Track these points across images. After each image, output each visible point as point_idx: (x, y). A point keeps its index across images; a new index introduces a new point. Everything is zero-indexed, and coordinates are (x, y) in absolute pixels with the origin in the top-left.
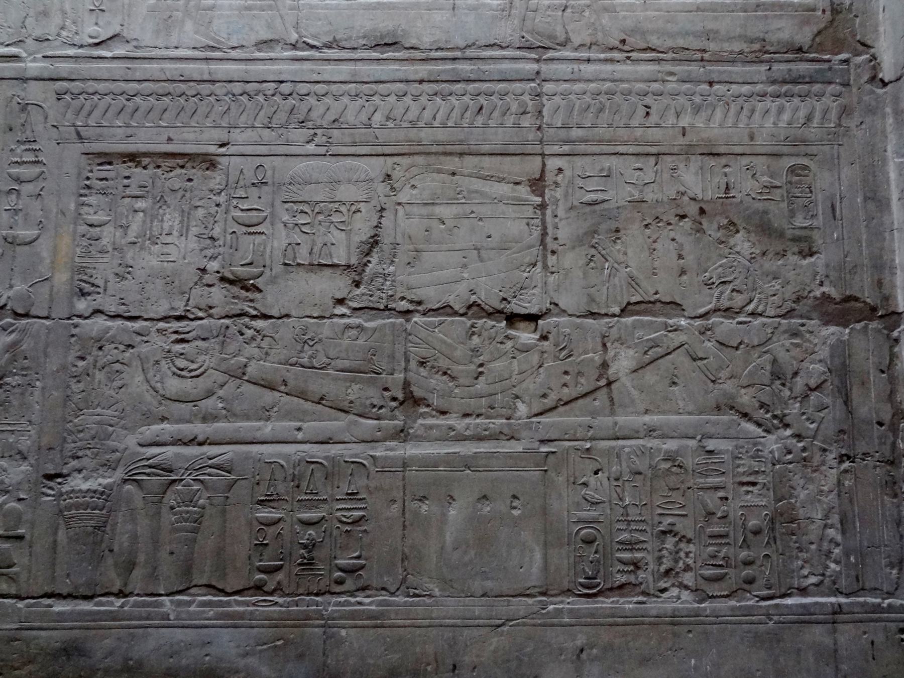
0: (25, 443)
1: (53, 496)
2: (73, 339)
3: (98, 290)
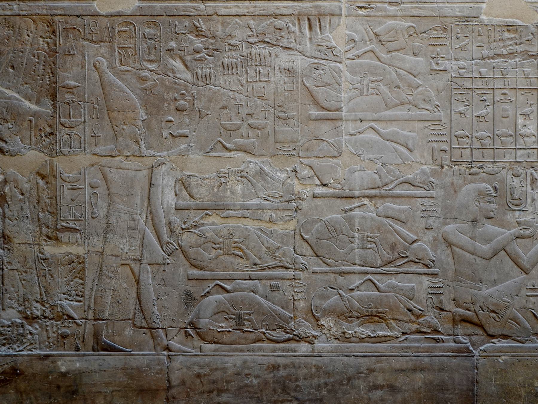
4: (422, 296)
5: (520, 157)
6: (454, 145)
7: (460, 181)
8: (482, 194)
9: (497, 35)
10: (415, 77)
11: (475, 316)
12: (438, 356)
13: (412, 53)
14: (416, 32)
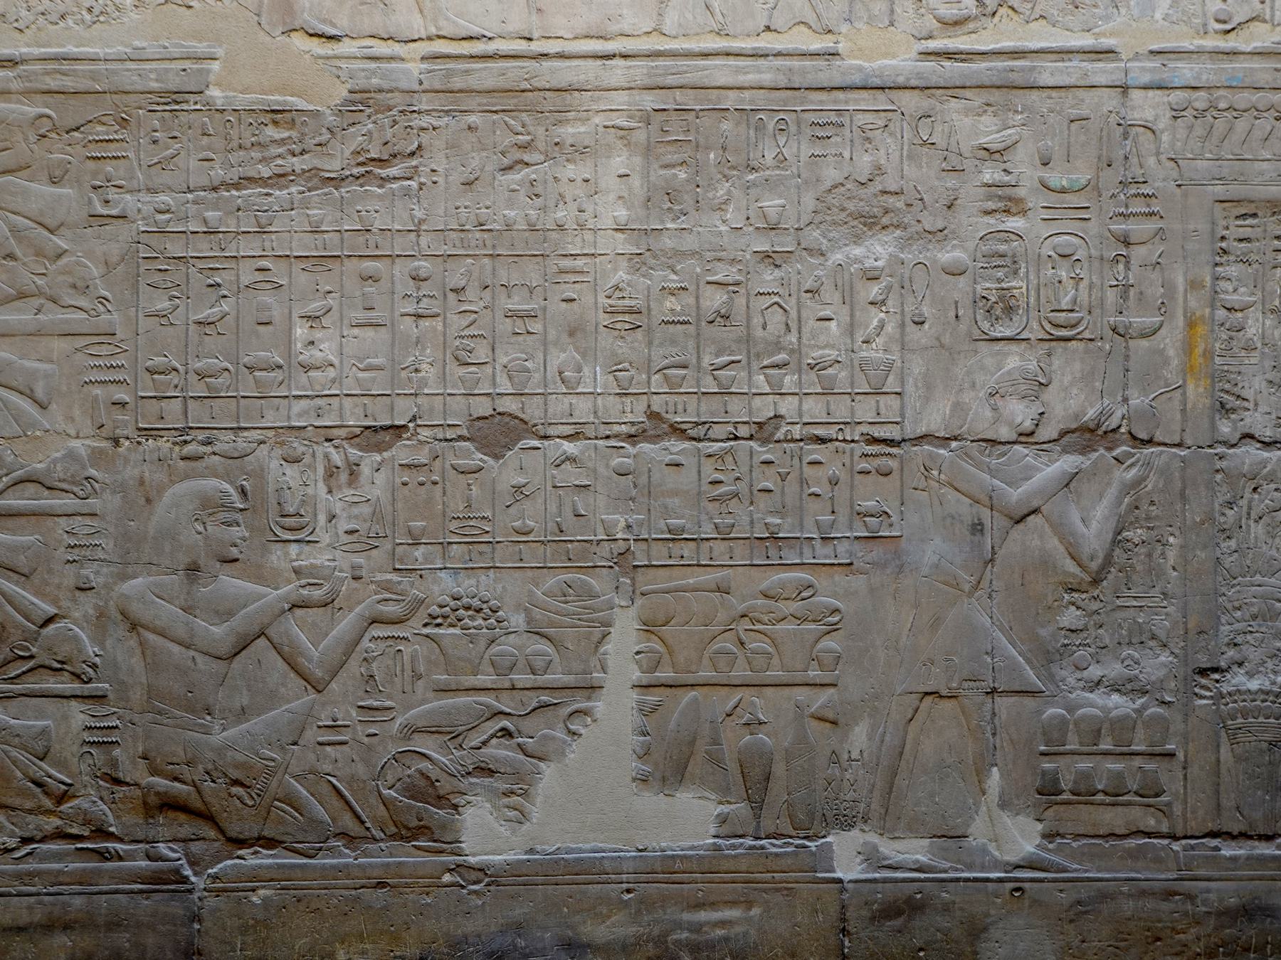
0: (1161, 624)
1: (1212, 697)
2: (1219, 477)
3: (1246, 404)
4: (69, 749)
5: (300, 415)
6: (143, 390)
7: (160, 476)
8: (210, 506)
9: (247, 134)
10: (51, 232)
11: (194, 795)
12: (106, 893)
13: (45, 178)
14: (54, 129)
